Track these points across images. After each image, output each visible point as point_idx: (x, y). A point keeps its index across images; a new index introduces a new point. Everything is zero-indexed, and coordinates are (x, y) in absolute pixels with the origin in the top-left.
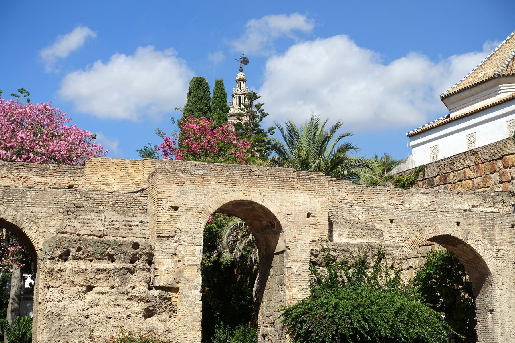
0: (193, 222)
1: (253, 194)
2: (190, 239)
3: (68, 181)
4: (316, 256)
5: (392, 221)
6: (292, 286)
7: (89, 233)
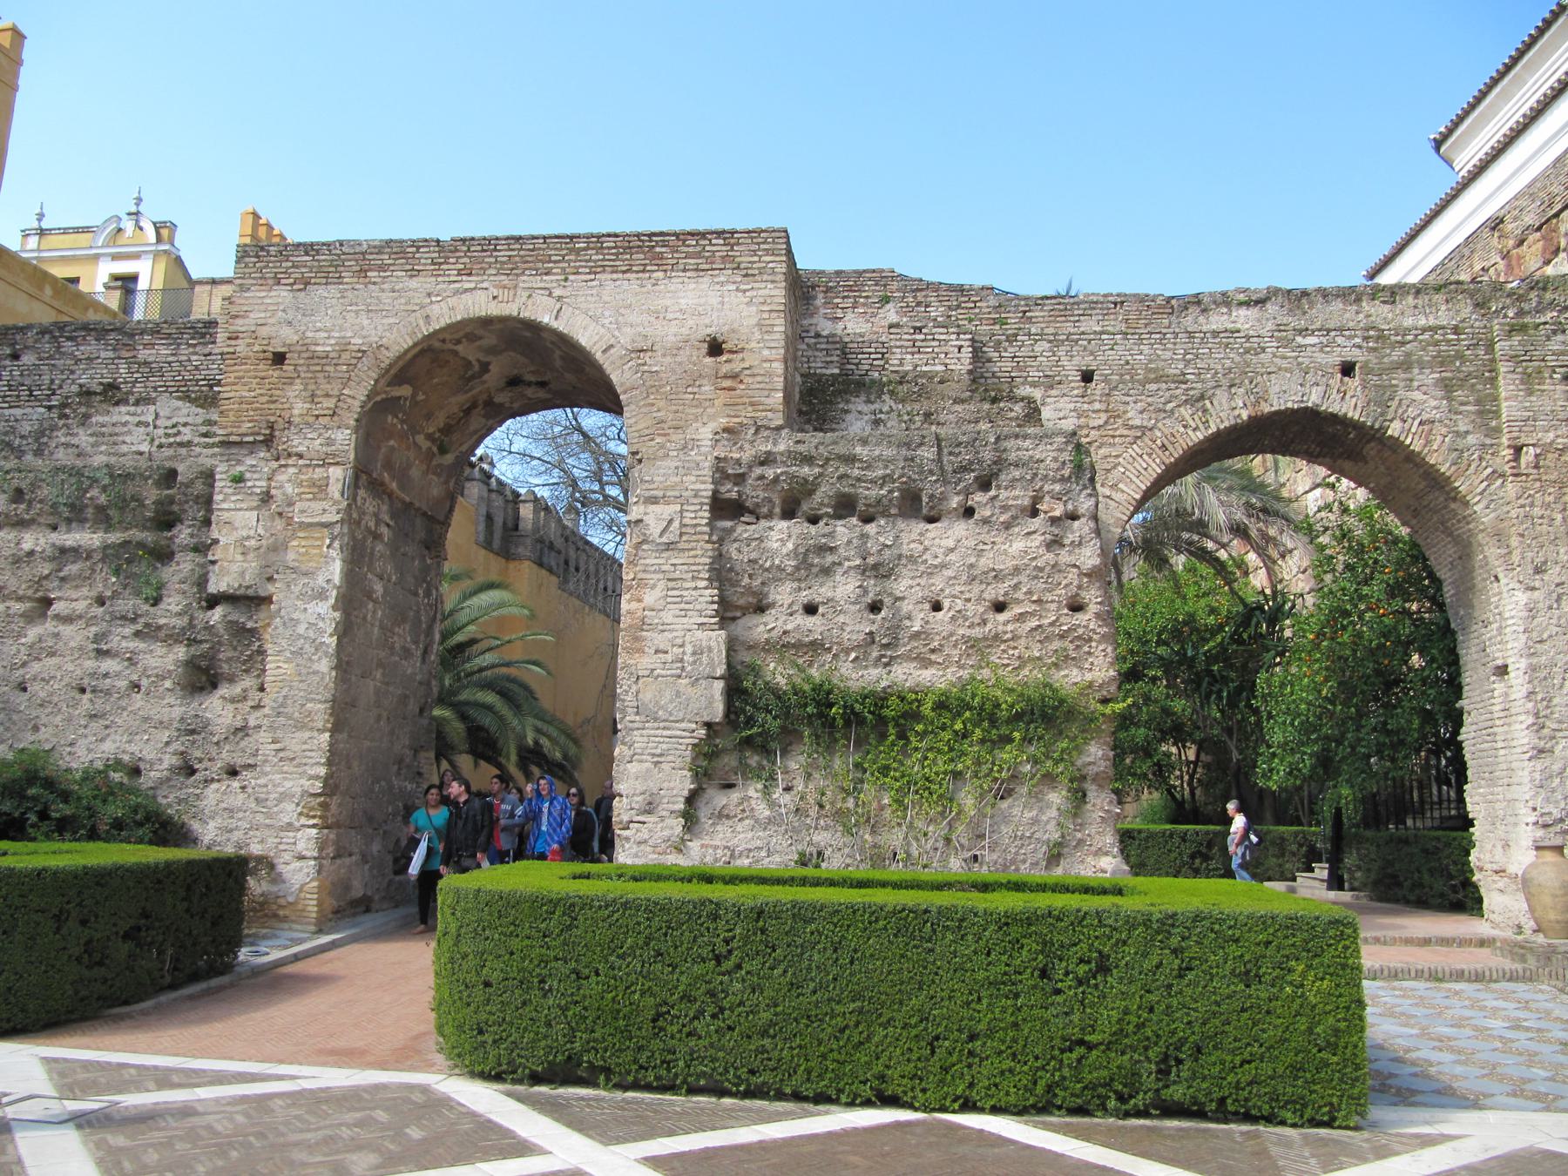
0: (327, 395)
4: (740, 479)
5: (1087, 377)
6: (642, 583)
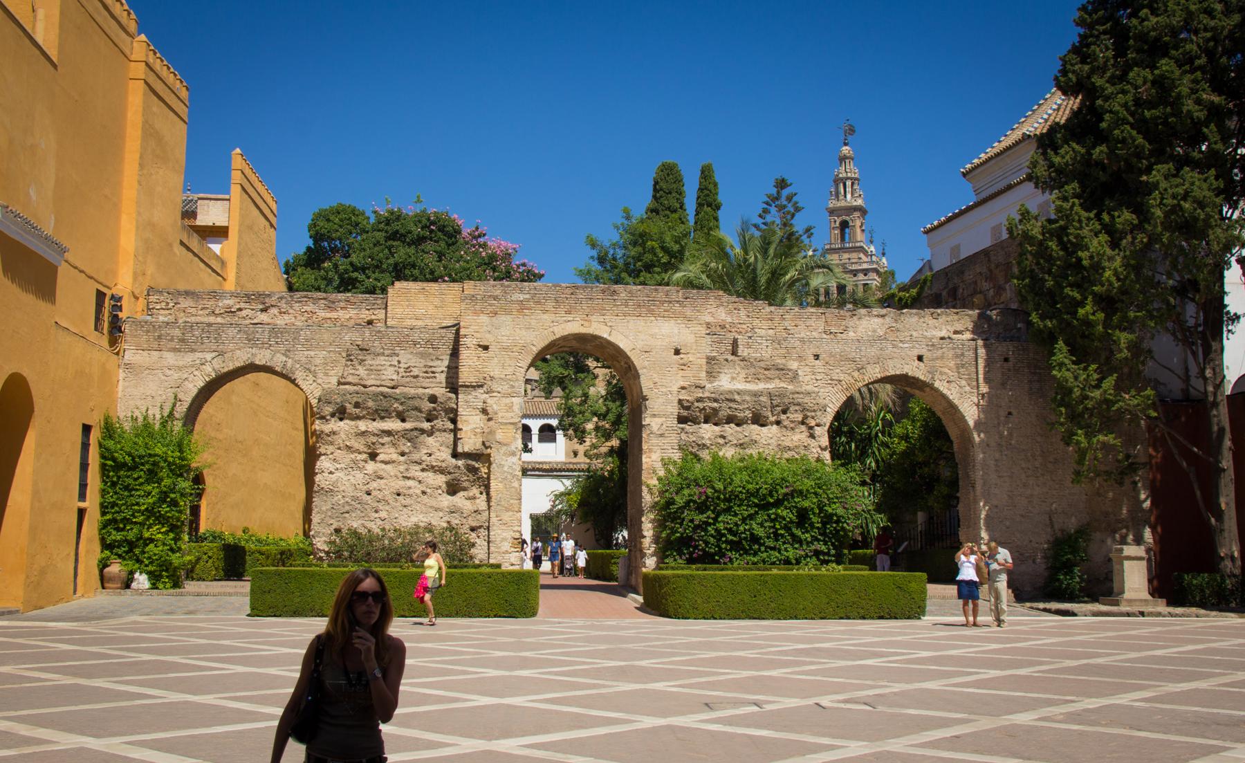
1: (595, 325)
2: (505, 388)
3: (366, 315)
4: (688, 408)
5: (817, 357)
6: (650, 451)
7: (378, 383)
